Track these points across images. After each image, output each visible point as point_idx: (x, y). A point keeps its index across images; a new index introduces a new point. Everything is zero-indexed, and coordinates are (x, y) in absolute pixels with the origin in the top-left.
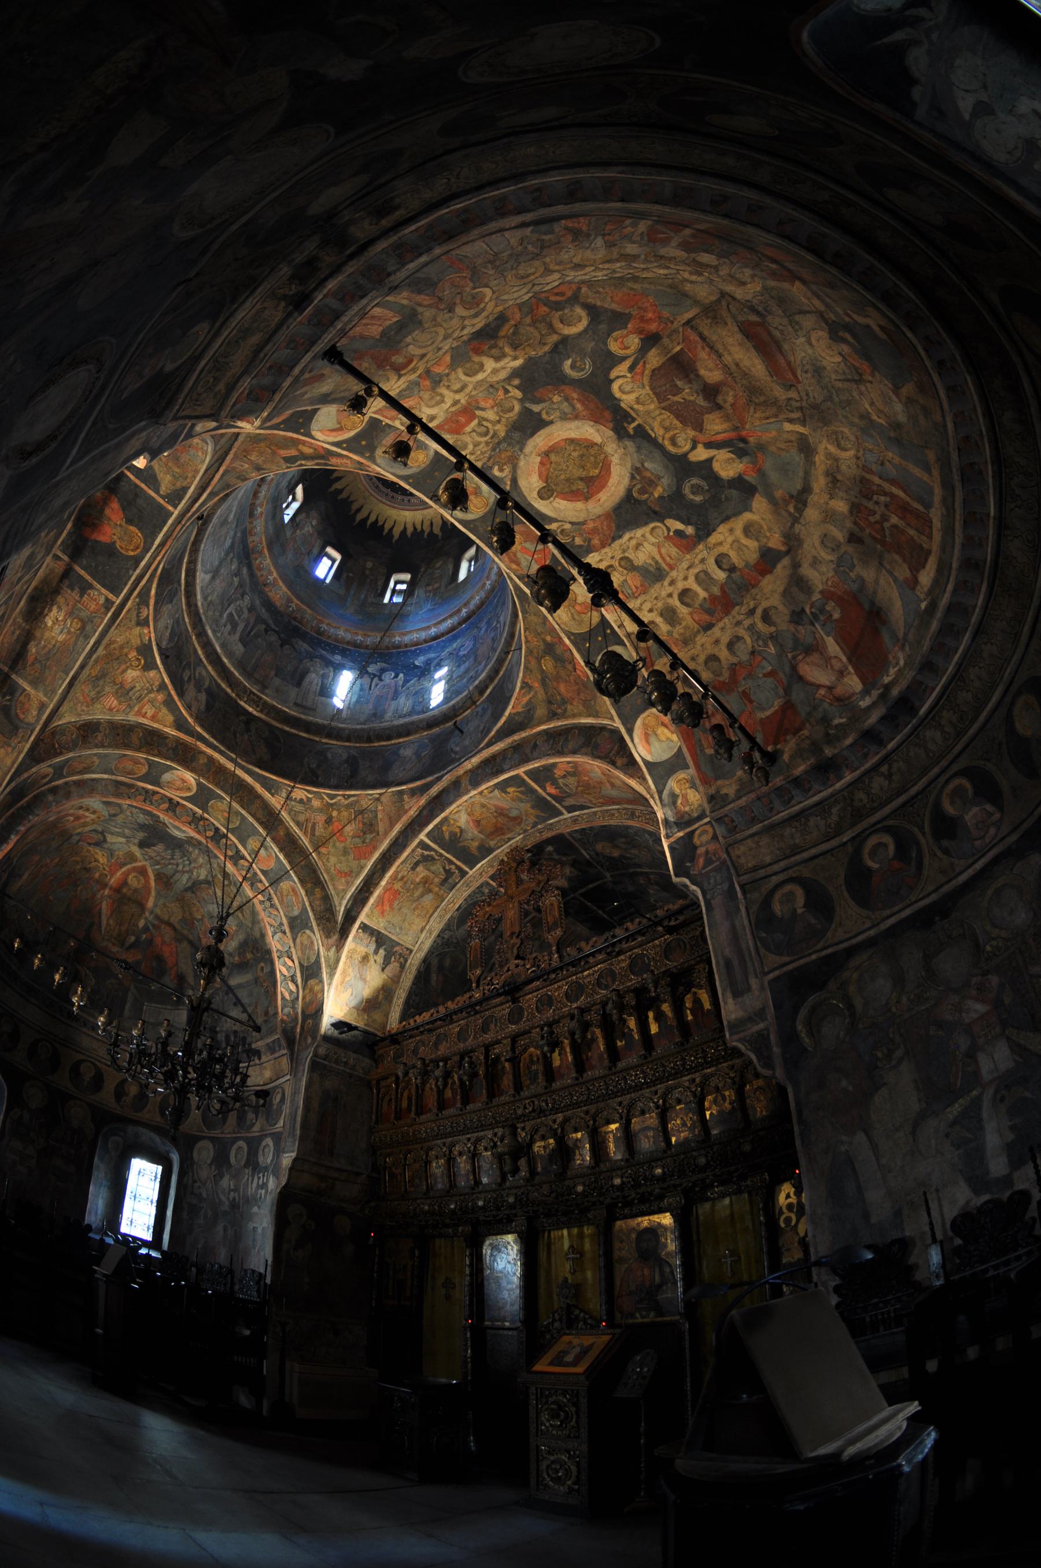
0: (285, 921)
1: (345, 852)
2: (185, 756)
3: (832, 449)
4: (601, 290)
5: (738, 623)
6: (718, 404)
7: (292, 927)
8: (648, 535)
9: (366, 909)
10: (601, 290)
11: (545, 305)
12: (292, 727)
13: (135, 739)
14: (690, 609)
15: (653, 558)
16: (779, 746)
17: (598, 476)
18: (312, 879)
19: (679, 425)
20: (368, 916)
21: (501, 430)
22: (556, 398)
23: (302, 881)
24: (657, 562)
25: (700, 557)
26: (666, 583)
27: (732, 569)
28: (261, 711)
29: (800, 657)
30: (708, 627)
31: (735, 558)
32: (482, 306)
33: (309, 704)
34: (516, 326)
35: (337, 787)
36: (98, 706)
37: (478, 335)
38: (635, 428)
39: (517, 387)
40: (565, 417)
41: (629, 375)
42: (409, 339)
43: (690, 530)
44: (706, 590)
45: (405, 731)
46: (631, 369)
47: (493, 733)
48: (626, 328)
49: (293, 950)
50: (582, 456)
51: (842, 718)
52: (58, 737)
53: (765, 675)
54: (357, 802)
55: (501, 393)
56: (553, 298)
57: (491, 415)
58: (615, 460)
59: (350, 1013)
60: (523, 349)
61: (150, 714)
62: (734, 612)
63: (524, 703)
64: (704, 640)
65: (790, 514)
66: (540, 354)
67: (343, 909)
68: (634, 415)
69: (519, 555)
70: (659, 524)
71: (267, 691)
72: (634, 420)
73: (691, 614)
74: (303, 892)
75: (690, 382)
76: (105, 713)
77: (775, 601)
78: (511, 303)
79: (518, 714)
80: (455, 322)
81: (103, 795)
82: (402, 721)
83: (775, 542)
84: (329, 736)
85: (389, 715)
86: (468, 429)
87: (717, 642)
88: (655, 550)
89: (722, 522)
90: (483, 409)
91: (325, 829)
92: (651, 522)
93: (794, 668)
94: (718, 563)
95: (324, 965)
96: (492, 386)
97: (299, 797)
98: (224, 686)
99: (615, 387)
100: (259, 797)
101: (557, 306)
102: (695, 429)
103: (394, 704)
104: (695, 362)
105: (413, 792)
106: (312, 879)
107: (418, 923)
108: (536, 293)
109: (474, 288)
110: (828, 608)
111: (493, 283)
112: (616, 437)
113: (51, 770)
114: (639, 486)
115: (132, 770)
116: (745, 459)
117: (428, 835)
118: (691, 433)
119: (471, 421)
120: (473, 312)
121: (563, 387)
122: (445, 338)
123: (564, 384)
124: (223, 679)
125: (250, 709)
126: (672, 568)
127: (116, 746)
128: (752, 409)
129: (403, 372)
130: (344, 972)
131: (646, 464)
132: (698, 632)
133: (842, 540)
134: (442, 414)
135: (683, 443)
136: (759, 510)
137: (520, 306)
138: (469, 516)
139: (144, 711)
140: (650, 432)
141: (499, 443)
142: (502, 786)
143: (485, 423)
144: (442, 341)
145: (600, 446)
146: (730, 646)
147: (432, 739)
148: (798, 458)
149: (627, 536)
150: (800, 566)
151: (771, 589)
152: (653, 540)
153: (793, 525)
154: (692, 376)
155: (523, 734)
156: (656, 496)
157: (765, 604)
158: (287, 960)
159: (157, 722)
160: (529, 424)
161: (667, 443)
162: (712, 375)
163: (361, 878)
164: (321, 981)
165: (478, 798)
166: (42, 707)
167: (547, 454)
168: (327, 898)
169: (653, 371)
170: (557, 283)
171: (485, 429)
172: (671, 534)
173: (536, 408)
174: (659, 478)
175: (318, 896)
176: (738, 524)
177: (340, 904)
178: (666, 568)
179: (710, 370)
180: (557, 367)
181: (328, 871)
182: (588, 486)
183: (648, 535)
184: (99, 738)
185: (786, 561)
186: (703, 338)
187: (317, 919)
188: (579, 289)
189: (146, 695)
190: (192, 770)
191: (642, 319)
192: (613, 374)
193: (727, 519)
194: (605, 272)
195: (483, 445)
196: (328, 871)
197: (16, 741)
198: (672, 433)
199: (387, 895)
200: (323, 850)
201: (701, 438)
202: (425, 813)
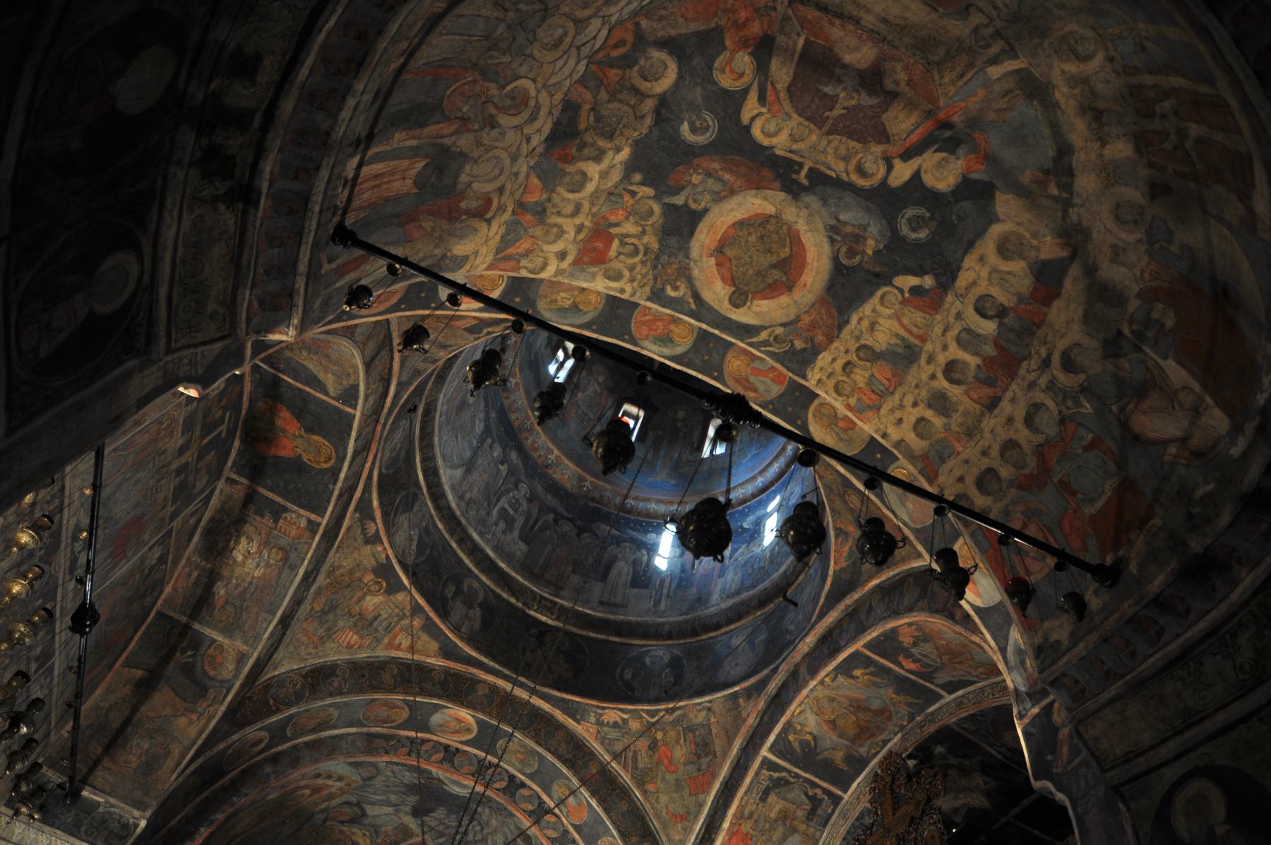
1: (678, 786)
2: (457, 689)
3: (1071, 68)
4: (663, 12)
5: (1032, 386)
6: (890, 92)
8: (879, 308)
11: (611, 67)
12: (599, 632)
13: (387, 678)
15: (897, 335)
16: (1121, 553)
17: (791, 256)
19: (859, 146)
22: (696, 179)
24: (903, 339)
25: (953, 312)
26: (923, 362)
27: (1002, 312)
28: (558, 619)
29: (1131, 406)
30: (992, 404)
31: (1002, 297)
32: (532, 103)
33: (619, 599)
34: (593, 109)
35: (657, 701)
36: (330, 645)
37: (555, 138)
38: (807, 176)
39: (643, 183)
40: (718, 198)
41: (764, 110)
42: (464, 178)
43: (928, 281)
44: (976, 354)
45: (736, 614)
46: (762, 100)
48: (725, 48)
50: (762, 238)
51: (1207, 483)
52: (273, 691)
53: (1086, 449)
54: (684, 715)
55: (627, 197)
56: (616, 53)
57: (629, 228)
58: (802, 226)
60: (621, 134)
61: (406, 643)
62: (1022, 372)
63: (845, 555)
64: (992, 422)
65: (1054, 199)
66: (645, 131)
68: (800, 160)
69: (752, 379)
70: (887, 289)
71: (563, 593)
72: (801, 165)
73: (966, 393)
75: (840, 81)
77: (1076, 334)
78: (567, 83)
80: (511, 136)
81: (349, 754)
82: (730, 602)
83: (1050, 248)
84: (646, 636)
85: (715, 597)
86: (612, 253)
87: (1010, 420)
88: (895, 323)
89: (966, 252)
90: (617, 225)
91: (651, 757)
92: (877, 289)
93: (1125, 425)
94: (980, 311)
96: (611, 194)
97: (612, 721)
98: (505, 596)
99: (756, 132)
100: (561, 727)
101: (627, 62)
102: (879, 142)
103: (720, 582)
104: (831, 50)
105: (749, 694)
108: (589, 57)
109: (503, 87)
110: (1155, 316)
111: (523, 70)
112: (790, 197)
113: (264, 734)
114: (844, 249)
115: (389, 717)
116: (961, 151)
117: (771, 749)
118: (878, 149)
119: (611, 243)
120: (525, 115)
121: (696, 161)
122: (514, 158)
123: (696, 156)
124: (502, 589)
125: (544, 619)
126: (923, 340)
127: (361, 691)
128: (936, 76)
129: (489, 216)
131: (842, 217)
132: (982, 414)
133: (1142, 201)
134: (571, 246)
135: (874, 167)
136: (1010, 214)
137: (582, 81)
138: (679, 350)
139: (397, 642)
140: (828, 172)
141: (657, 258)
142: (845, 669)
143: (627, 240)
144: (512, 164)
145: (777, 217)
146: (1029, 420)
147: (766, 620)
148: (1028, 110)
149: (854, 319)
150: (1096, 269)
151: (1065, 319)
152: (888, 312)
153: (1065, 212)
154: (838, 71)
155: (856, 595)
156: (870, 252)
157: (1061, 345)
159: (418, 652)
160: (681, 223)
162: (860, 55)
165: (821, 692)
166: (242, 658)
167: (719, 250)
169: (789, 89)
170: (604, 32)
171: (632, 248)
172: (907, 295)
173: (679, 200)
176: (988, 246)
179: (856, 49)
180: (676, 139)
181: (658, 816)
182: (784, 274)
183: (879, 308)
184: (336, 684)
185: (1075, 270)
188: (637, 24)
189: (397, 622)
190: (468, 705)
191: (739, 26)
193: (971, 245)
195: (639, 267)
196: (658, 816)
197: (204, 705)
198: (854, 162)
200: (651, 788)
201: (893, 149)
202: (766, 718)
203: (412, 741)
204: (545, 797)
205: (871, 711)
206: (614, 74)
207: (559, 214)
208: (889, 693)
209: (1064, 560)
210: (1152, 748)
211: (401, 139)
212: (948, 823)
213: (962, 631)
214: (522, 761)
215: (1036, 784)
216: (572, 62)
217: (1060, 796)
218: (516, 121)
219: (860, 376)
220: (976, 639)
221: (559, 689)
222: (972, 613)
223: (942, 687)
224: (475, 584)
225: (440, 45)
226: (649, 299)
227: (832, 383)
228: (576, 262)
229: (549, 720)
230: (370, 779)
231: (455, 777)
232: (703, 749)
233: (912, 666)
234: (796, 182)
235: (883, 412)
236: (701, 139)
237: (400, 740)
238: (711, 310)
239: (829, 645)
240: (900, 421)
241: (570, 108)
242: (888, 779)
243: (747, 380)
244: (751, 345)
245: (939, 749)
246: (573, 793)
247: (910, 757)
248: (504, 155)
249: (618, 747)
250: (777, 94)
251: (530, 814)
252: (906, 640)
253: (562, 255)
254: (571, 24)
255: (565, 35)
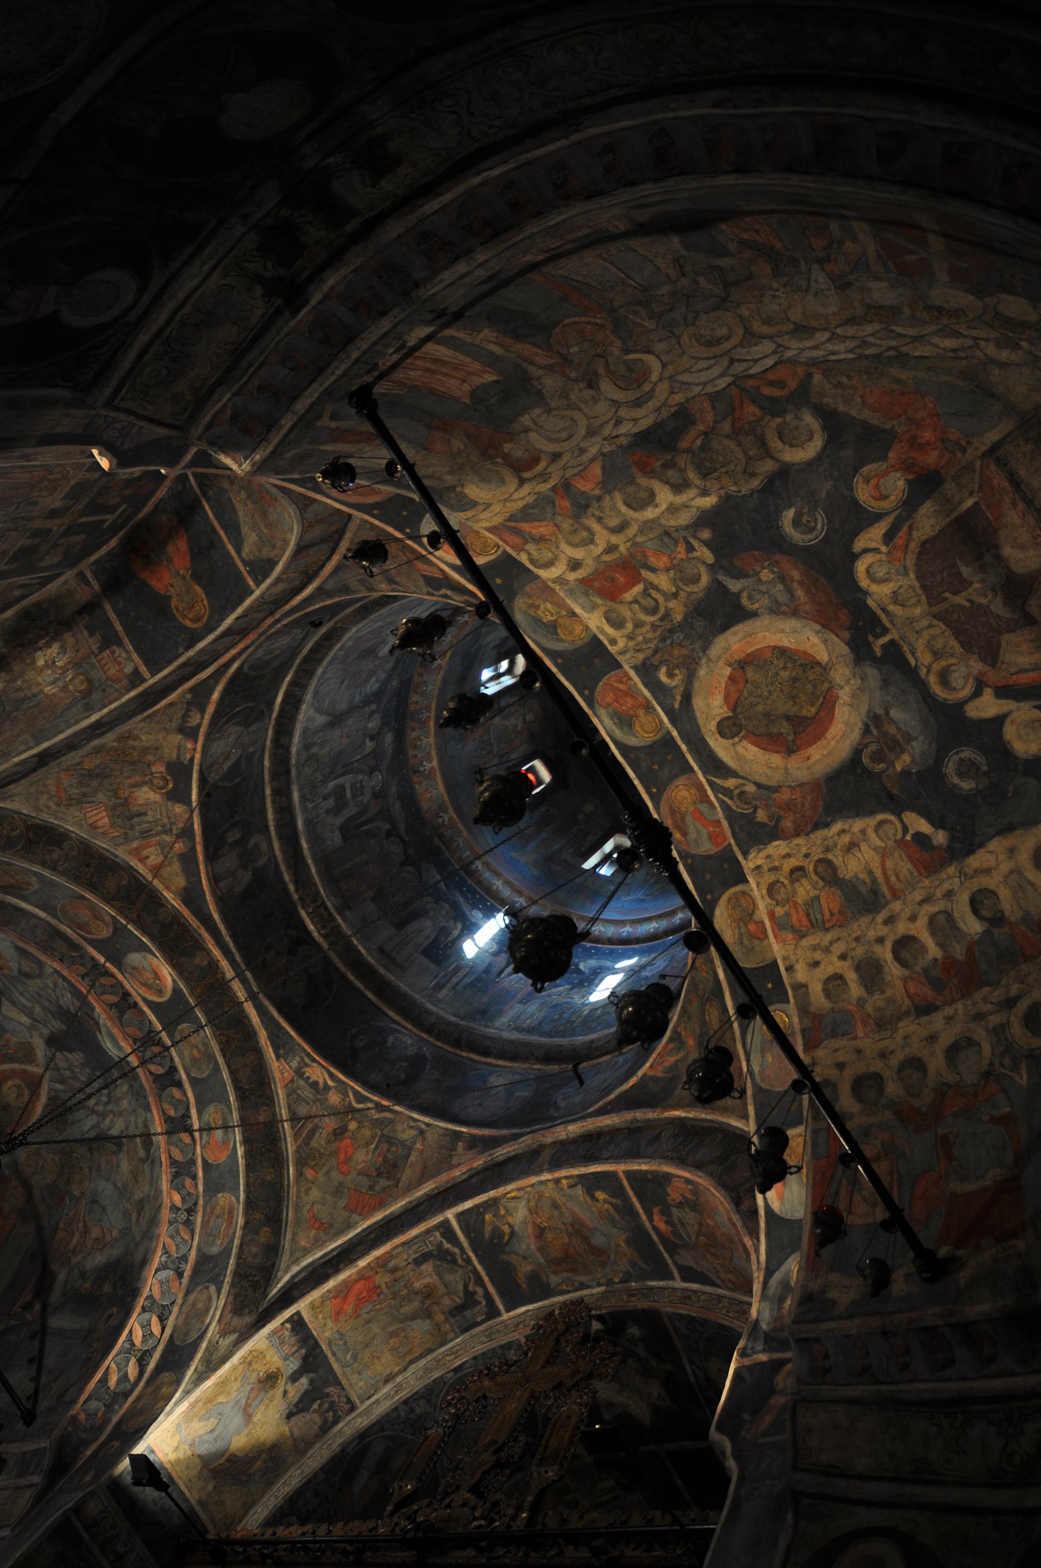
0: (193, 1256)
2: (177, 943)
4: (845, 380)
5: (979, 1017)
7: (196, 1272)
8: (870, 832)
9: (316, 1295)
10: (845, 380)
14: (906, 972)
15: (870, 873)
18: (268, 1207)
20: (312, 1306)
21: (678, 610)
22: (766, 575)
23: (249, 1204)
24: (874, 880)
25: (946, 886)
26: (880, 918)
27: (997, 920)
28: (325, 937)
30: (925, 1009)
32: (647, 387)
35: (373, 1088)
39: (706, 544)
40: (776, 610)
41: (884, 549)
42: (526, 420)
43: (940, 838)
44: (941, 945)
45: (513, 1052)
46: (889, 537)
47: (612, 1096)
48: (885, 458)
49: (175, 1310)
50: (795, 680)
53: (993, 1120)
54: (392, 1122)
55: (681, 548)
56: (767, 391)
57: (663, 581)
58: (844, 695)
59: (185, 1463)
61: (154, 860)
62: (978, 996)
63: (667, 1064)
64: (913, 1028)
67: (286, 1278)
69: (689, 820)
70: (892, 818)
71: (348, 914)
72: (885, 631)
73: (905, 980)
74: (241, 1221)
75: (983, 569)
76: (81, 827)
79: (655, 1079)
80: (602, 408)
84: (405, 1013)
86: (628, 596)
87: (932, 1038)
88: (877, 859)
90: (653, 570)
91: (329, 1142)
94: (975, 904)
95: (199, 1355)
96: (667, 533)
97: (314, 1078)
98: (286, 877)
99: (861, 567)
100: (258, 1051)
101: (773, 407)
106: (268, 1207)
107: (386, 1363)
108: (737, 377)
117: (459, 1216)
118: (977, 666)
120: (631, 395)
122: (591, 432)
124: (289, 868)
125: (311, 927)
126: (896, 895)
127: (76, 879)
130: (223, 1383)
131: (893, 713)
132: (907, 1013)
138: (632, 741)
139: (145, 853)
140: (909, 657)
141: (672, 631)
142: (591, 1183)
145: (825, 669)
146: (953, 1052)
147: (540, 1078)
149: (837, 827)
152: (878, 842)
154: (988, 558)
155: (651, 1115)
156: (899, 768)
158: (155, 1320)
160: (720, 611)
161: (932, 679)
163: (339, 1242)
164: (178, 1382)
165: (549, 1191)
167: (741, 665)
168: (273, 1250)
169: (924, 544)
170: (770, 362)
172: (908, 838)
173: (734, 585)
174: (909, 739)
175: (262, 1239)
177: (287, 1269)
178: (886, 893)
179: (1023, 548)
181: (298, 1208)
182: (794, 732)
183: (870, 832)
184: (55, 856)
186: (1016, 483)
187: (236, 1274)
188: (810, 375)
189: (159, 833)
192: (859, 545)
193: (1009, 829)
194: (850, 344)
196: (298, 1208)
199: (359, 1286)
200: (309, 1173)
201: (994, 677)
202: (474, 1180)
203: (95, 964)
204: (193, 1112)
205: (589, 1243)
206: (751, 411)
207: (600, 520)
208: (620, 1238)
209: (895, 1220)
210: (861, 1477)
211: (487, 338)
212: (594, 1413)
213: (739, 1224)
214: (194, 1059)
215: (714, 1435)
216: (716, 371)
217: (731, 1464)
218: (618, 395)
219: (804, 891)
220: (749, 1243)
221: (280, 1011)
222: (762, 1212)
223: (681, 1268)
224: (264, 846)
225: (590, 267)
226: (635, 668)
227: (770, 878)
228: (583, 581)
229: (250, 1035)
230: (27, 976)
231: (115, 1031)
232: (389, 1170)
233: (662, 1226)
234: (869, 646)
235: (804, 942)
236: (797, 537)
237: (84, 955)
238: (693, 720)
239: (589, 1147)
240: (816, 964)
241: (683, 417)
242: (561, 1327)
243: (683, 818)
244: (711, 784)
245: (634, 1331)
246: (226, 1127)
247: (600, 1318)
248: (583, 422)
249: (303, 1110)
250: (909, 540)
251: (168, 1119)
252: (674, 1194)
253: (575, 565)
254: (740, 332)
255: (728, 338)
